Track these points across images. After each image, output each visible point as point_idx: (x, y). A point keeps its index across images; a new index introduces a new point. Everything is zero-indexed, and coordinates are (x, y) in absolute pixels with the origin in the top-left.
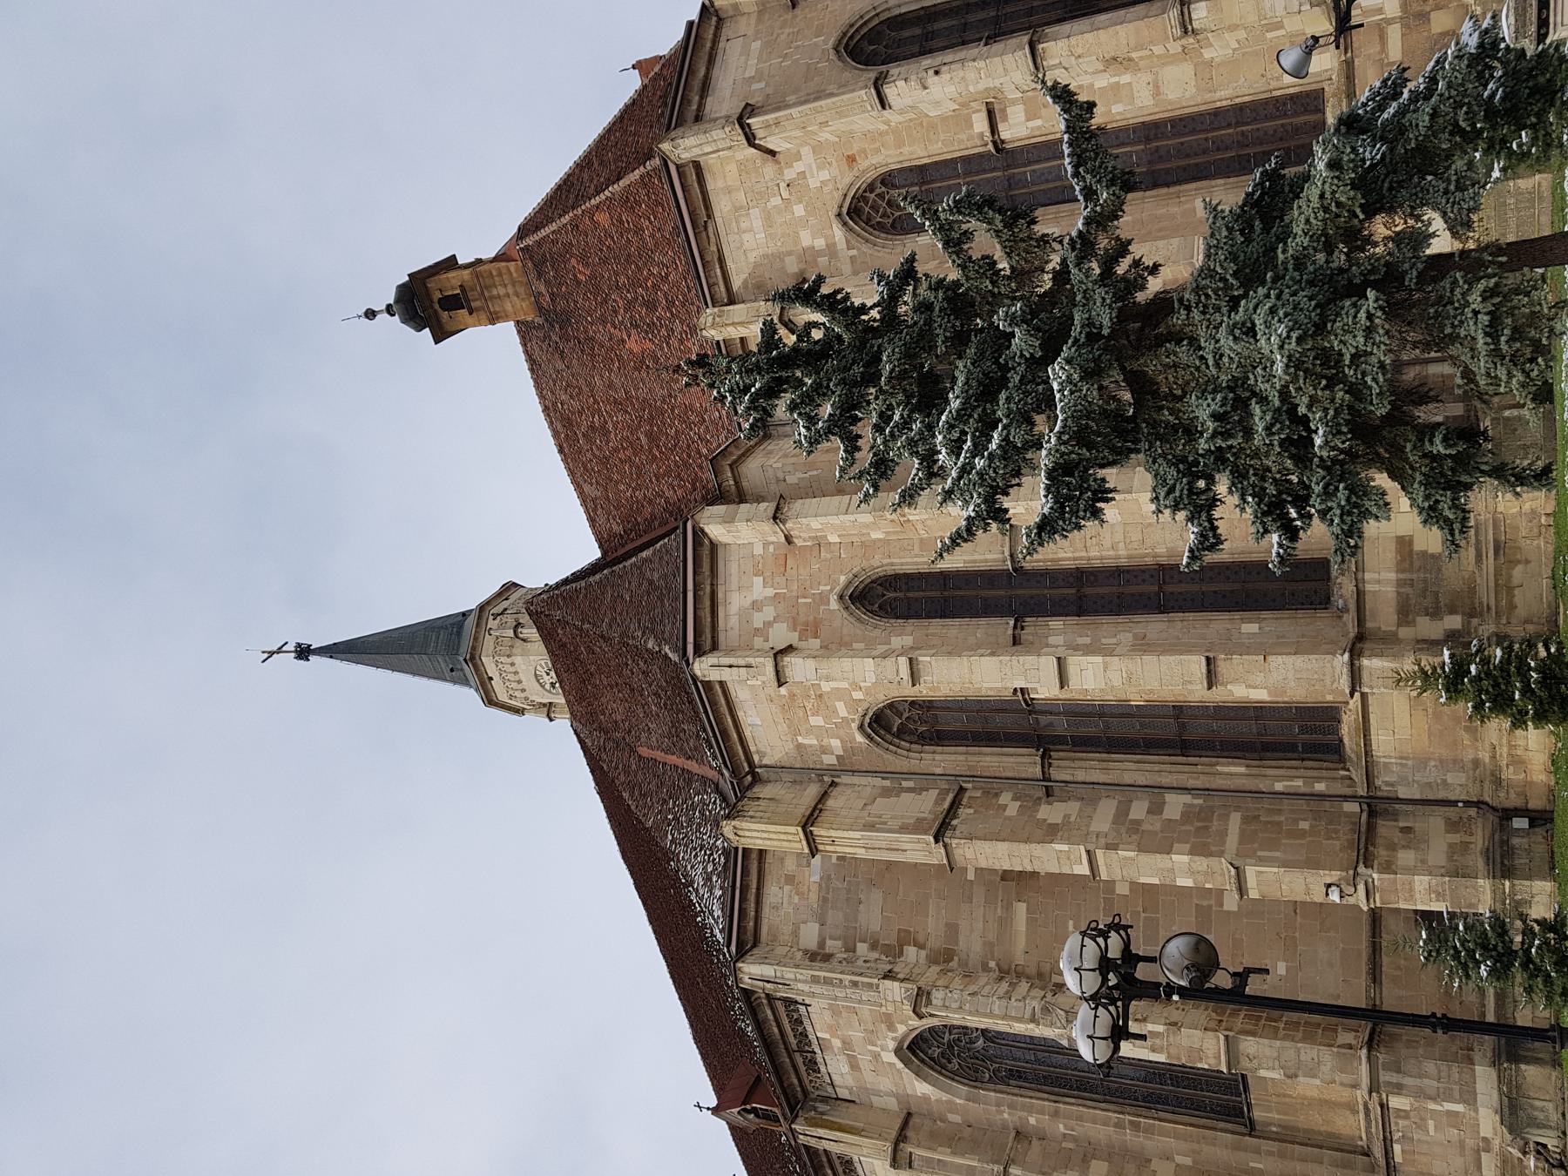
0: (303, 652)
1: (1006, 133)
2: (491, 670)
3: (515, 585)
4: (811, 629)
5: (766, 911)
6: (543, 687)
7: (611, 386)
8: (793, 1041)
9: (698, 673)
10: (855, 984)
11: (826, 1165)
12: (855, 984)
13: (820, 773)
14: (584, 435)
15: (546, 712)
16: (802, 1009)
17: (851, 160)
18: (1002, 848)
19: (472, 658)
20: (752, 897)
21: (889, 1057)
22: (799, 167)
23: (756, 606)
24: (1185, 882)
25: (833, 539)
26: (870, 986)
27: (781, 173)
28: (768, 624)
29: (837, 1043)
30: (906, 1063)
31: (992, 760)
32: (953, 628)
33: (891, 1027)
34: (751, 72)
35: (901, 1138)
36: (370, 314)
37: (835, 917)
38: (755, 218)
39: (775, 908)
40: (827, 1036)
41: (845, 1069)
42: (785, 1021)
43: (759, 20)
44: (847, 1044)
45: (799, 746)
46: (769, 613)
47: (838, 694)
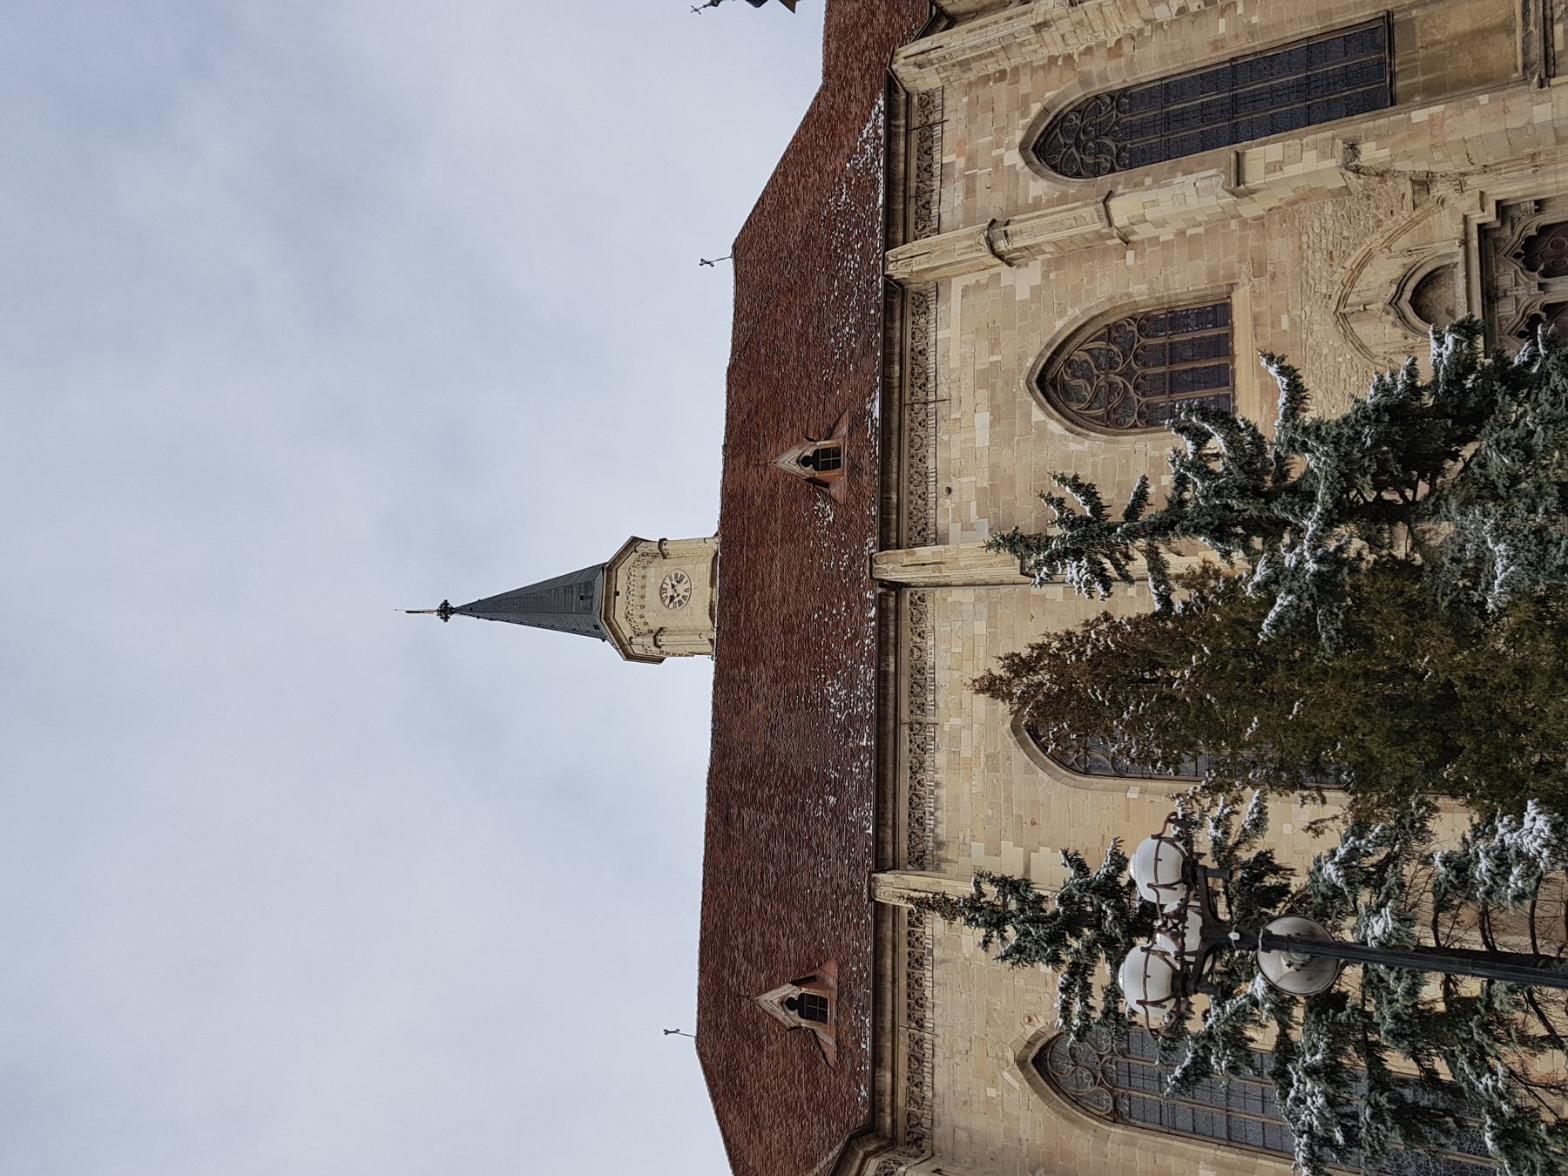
0: (445, 611)
6: (663, 602)
8: (913, 184)
10: (1010, 18)
11: (897, 358)
21: (1013, 158)
30: (1028, 163)
42: (914, 163)
44: (971, 161)
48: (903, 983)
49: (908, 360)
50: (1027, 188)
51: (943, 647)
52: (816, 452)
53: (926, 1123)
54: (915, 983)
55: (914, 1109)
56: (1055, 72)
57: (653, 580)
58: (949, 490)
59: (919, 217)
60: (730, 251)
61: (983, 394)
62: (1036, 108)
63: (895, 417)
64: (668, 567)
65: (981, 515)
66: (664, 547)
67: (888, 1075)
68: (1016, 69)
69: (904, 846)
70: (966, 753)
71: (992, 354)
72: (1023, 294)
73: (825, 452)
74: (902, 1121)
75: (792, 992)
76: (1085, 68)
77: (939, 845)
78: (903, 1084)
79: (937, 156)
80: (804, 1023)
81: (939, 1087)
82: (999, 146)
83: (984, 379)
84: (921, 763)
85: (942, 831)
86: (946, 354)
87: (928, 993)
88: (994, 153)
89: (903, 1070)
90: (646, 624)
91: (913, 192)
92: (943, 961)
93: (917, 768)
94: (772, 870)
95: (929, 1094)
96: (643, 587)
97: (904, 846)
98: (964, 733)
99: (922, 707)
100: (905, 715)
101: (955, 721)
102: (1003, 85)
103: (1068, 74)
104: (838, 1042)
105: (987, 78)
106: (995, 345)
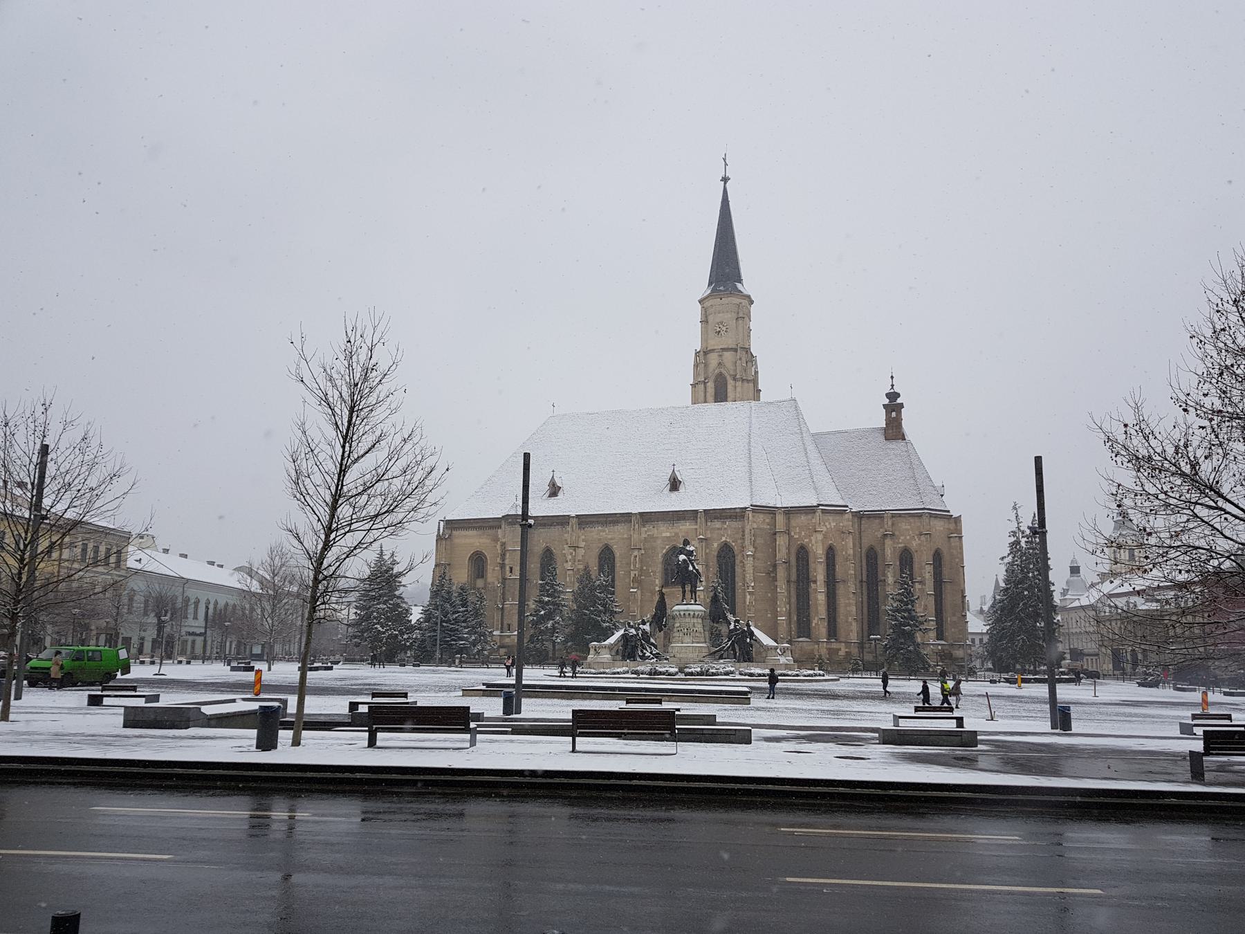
0: (725, 180)
1: (916, 584)
3: (752, 302)
4: (825, 537)
5: (757, 514)
16: (735, 520)
17: (917, 551)
18: (783, 575)
21: (724, 539)
22: (917, 540)
23: (830, 524)
24: (779, 609)
25: (843, 543)
26: (751, 543)
27: (917, 535)
28: (826, 526)
29: (725, 526)
31: (794, 570)
32: (825, 567)
33: (733, 542)
34: (937, 528)
36: (892, 377)
38: (909, 527)
41: (717, 526)
43: (948, 529)
44: (725, 529)
47: (811, 540)
51: (622, 527)
56: (740, 548)
58: (654, 527)
61: (673, 534)
62: (734, 544)
65: (648, 535)
68: (743, 539)
76: (740, 555)
77: (584, 529)
83: (677, 534)
85: (586, 529)
89: (542, 522)
93: (598, 522)
96: (723, 312)
100: (608, 519)
105: (743, 532)
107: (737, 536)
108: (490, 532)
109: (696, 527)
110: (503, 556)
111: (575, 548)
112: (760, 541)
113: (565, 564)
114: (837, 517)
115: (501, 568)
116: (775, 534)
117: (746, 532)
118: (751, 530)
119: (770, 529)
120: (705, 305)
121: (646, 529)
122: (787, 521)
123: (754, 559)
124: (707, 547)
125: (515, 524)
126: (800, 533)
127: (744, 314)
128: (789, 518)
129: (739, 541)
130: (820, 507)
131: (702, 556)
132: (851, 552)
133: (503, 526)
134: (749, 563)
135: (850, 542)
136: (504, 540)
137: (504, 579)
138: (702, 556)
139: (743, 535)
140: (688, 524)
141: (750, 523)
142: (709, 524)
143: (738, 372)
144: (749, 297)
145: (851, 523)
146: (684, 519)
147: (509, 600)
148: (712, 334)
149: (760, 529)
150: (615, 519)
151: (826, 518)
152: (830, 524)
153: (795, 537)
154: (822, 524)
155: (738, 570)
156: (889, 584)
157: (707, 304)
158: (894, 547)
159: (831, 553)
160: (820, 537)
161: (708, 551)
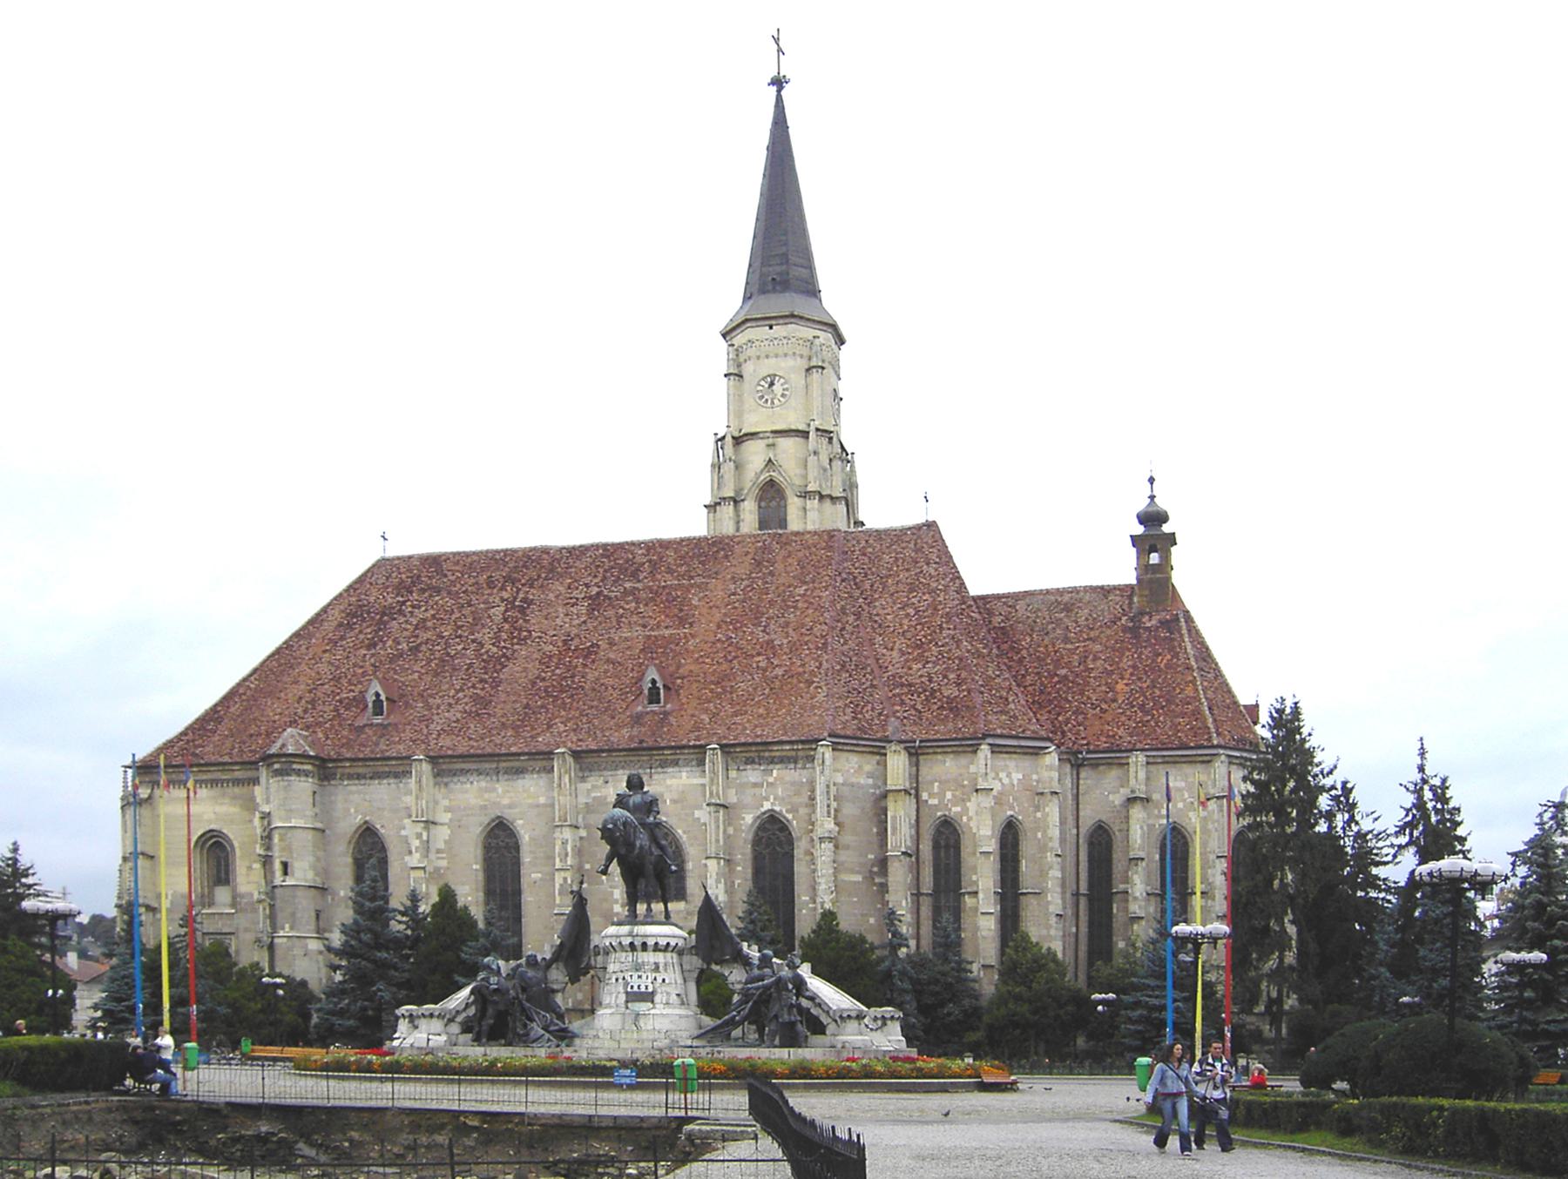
2: (779, 330)
5: (846, 755)
7: (1095, 659)
8: (767, 754)
9: (982, 747)
10: (828, 806)
12: (828, 806)
13: (917, 789)
14: (1061, 619)
15: (731, 371)
16: (792, 766)
19: (793, 316)
20: (852, 748)
21: (767, 806)
23: (1009, 775)
26: (829, 813)
28: (1000, 780)
30: (764, 813)
35: (725, 807)
37: (846, 790)
39: (847, 760)
40: (775, 775)
41: (752, 780)
45: (932, 783)
46: (1006, 781)
47: (966, 810)
48: (387, 769)
49: (673, 757)
50: (749, 813)
52: (658, 688)
53: (332, 782)
54: (387, 775)
55: (338, 776)
57: (783, 365)
58: (607, 782)
59: (747, 759)
60: (930, 519)
62: (790, 816)
63: (644, 753)
64: (798, 379)
66: (814, 370)
67: (348, 764)
68: (813, 805)
69: (444, 767)
70: (486, 796)
71: (671, 800)
72: (697, 814)
73: (659, 694)
74: (333, 770)
75: (383, 697)
77: (446, 784)
78: (347, 771)
79: (778, 766)
80: (370, 705)
81: (349, 788)
82: (775, 799)
84: (480, 774)
85: (452, 786)
86: (674, 777)
87: (385, 781)
88: (772, 797)
89: (351, 771)
90: (745, 361)
91: (762, 754)
92: (398, 787)
94: (460, 647)
95: (346, 783)
96: (777, 356)
97: (444, 767)
98: (494, 795)
99: (506, 773)
100: (503, 765)
101: (500, 790)
102: (805, 799)
103: (802, 831)
104: (365, 726)
105: (813, 791)
106: (674, 801)
107: (796, 800)
108: (237, 790)
109: (702, 781)
110: (267, 838)
111: (429, 823)
112: (849, 810)
113: (407, 858)
114: (1026, 762)
115: (264, 864)
116: (885, 797)
117: (818, 792)
118: (828, 786)
119: (875, 786)
120: (735, 341)
121: (588, 785)
122: (915, 768)
123: (836, 847)
124: (729, 822)
125: (288, 775)
126: (942, 795)
127: (823, 361)
128: (917, 765)
129: (803, 811)
130: (990, 741)
131: (717, 841)
132: (1055, 832)
133: (263, 780)
134: (824, 852)
135: (1052, 811)
136: (266, 809)
137: (273, 889)
138: (717, 841)
139: (812, 799)
140: (684, 774)
141: (827, 772)
142: (733, 774)
143: (811, 477)
144: (833, 328)
145: (1055, 775)
146: (676, 763)
147: (283, 929)
148: (750, 401)
149: (852, 785)
150: (517, 764)
151: (1002, 763)
152: (1009, 775)
153: (930, 802)
154: (991, 775)
155: (800, 868)
156: (1136, 898)
157: (739, 339)
158: (1148, 825)
159: (1010, 837)
160: (987, 801)
161: (731, 830)
